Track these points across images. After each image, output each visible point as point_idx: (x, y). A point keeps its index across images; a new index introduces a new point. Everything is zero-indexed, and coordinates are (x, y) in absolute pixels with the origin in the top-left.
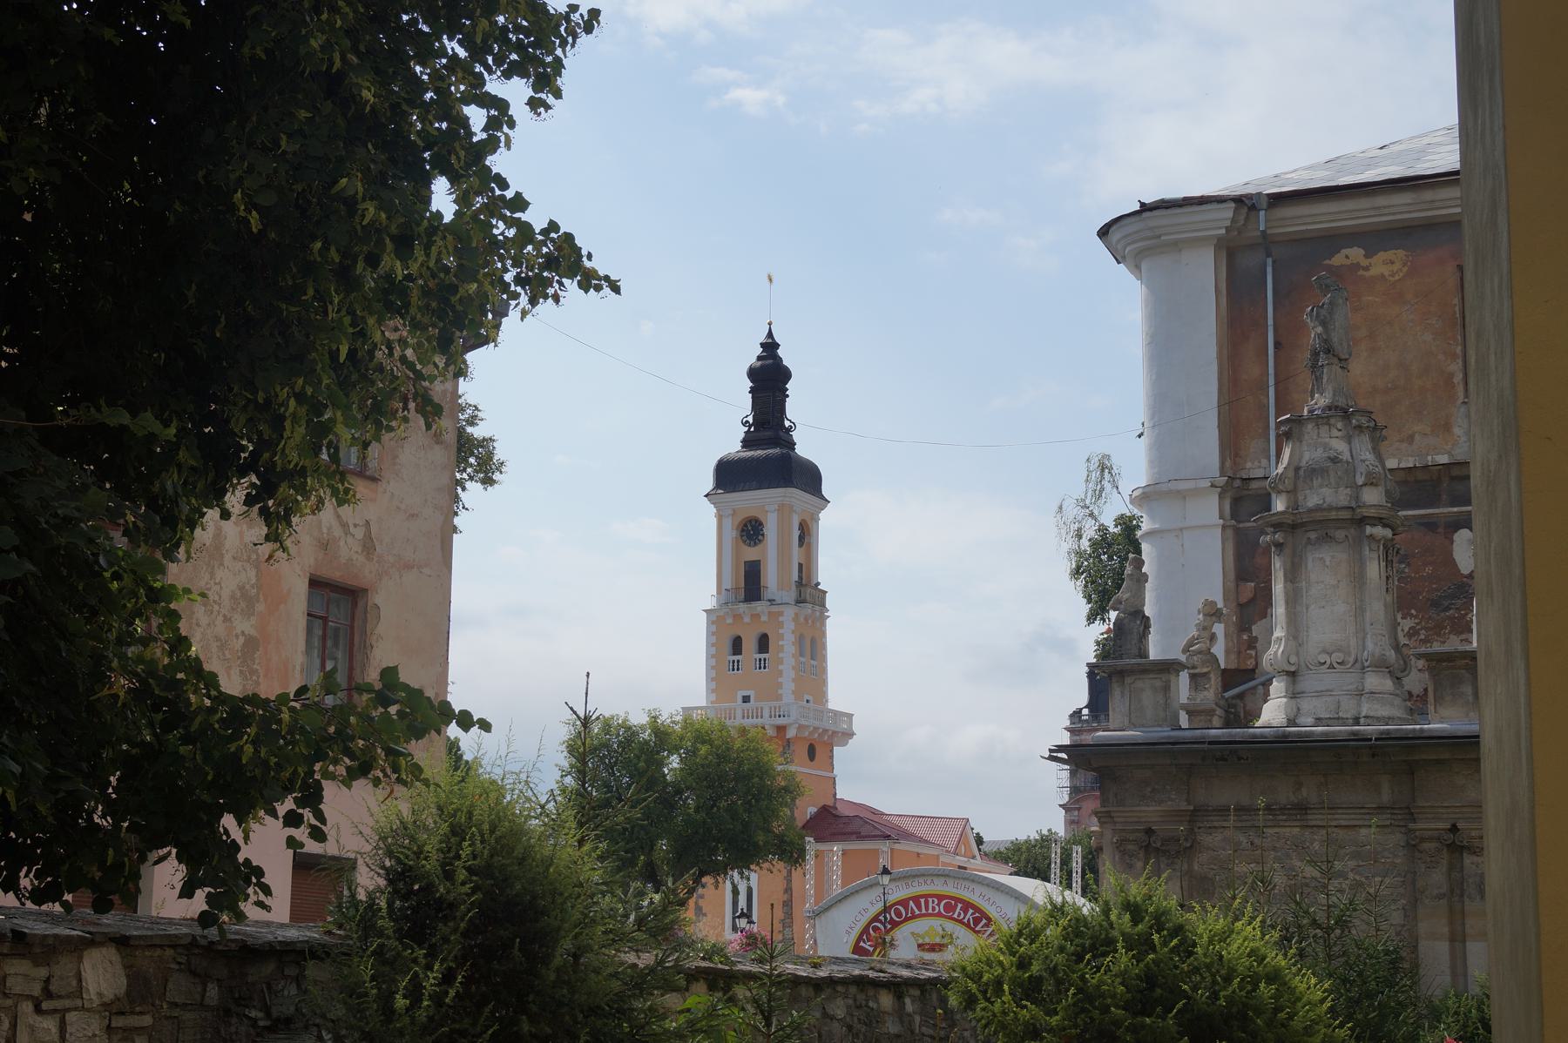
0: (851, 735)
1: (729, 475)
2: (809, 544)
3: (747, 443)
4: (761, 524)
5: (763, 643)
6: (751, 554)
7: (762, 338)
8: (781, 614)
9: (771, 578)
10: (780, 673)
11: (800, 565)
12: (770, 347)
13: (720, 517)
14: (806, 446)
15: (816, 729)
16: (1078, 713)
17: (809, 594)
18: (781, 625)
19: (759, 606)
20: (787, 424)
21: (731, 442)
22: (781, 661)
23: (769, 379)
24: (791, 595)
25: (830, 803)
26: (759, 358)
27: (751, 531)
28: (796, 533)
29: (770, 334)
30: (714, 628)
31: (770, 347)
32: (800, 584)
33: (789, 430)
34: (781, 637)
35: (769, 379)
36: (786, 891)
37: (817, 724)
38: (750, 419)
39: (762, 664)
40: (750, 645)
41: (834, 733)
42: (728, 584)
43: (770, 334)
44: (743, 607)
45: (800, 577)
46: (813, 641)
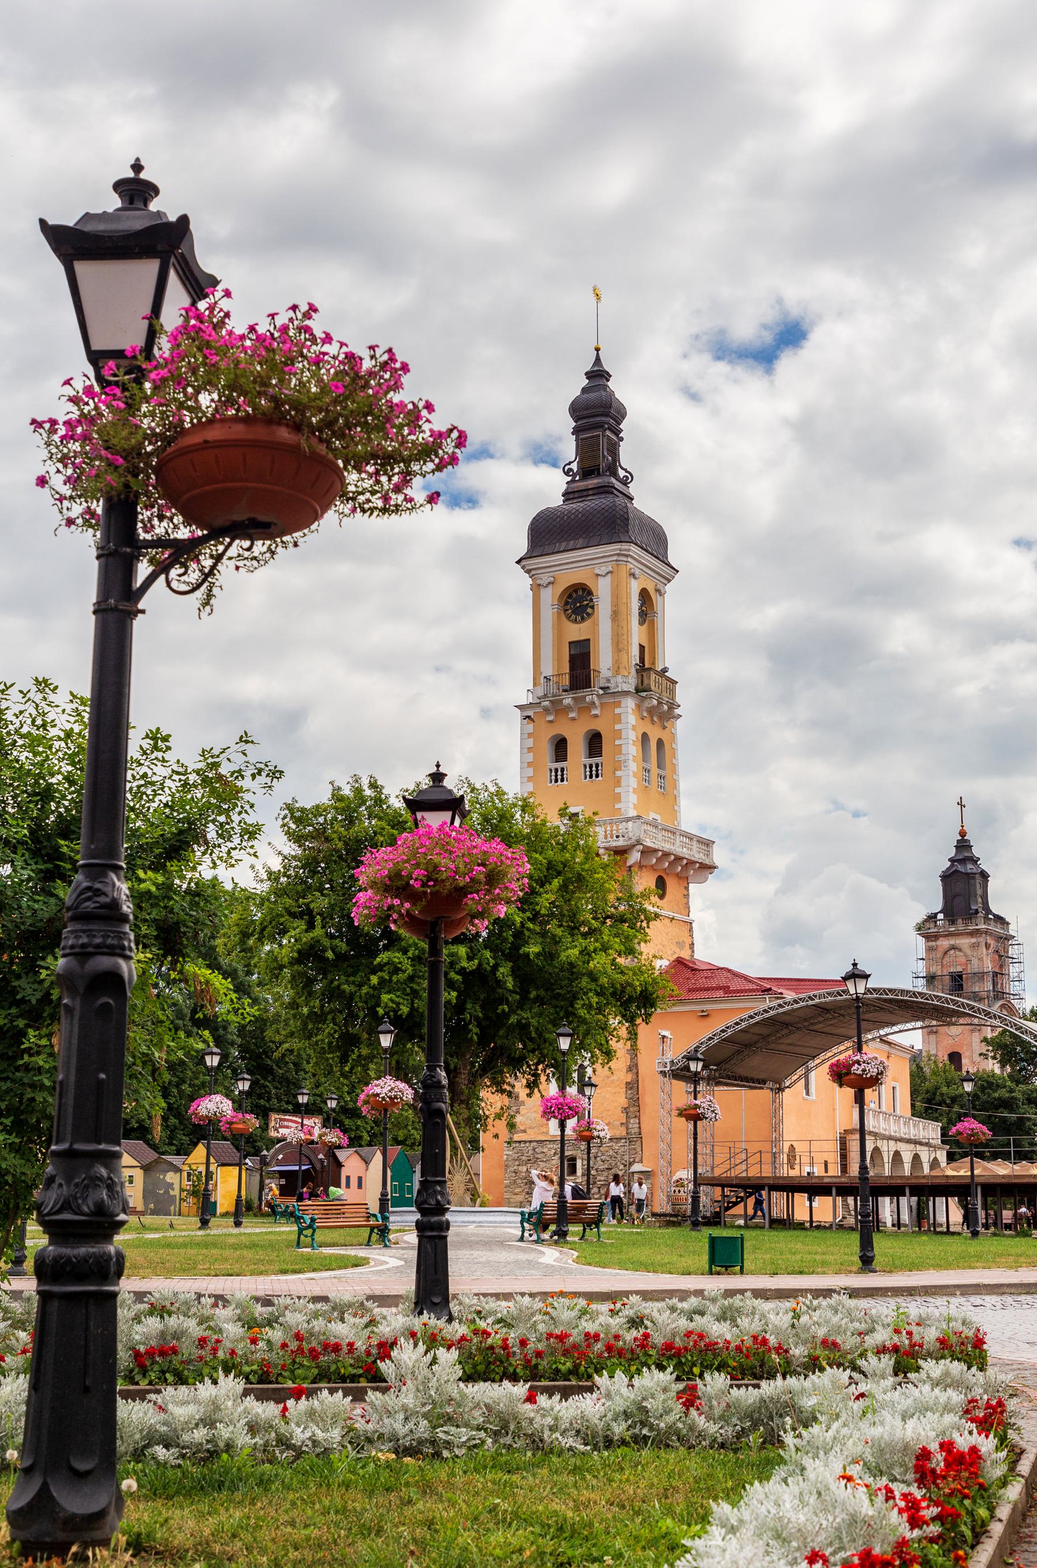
0: (710, 868)
1: (548, 534)
2: (652, 624)
3: (568, 495)
4: (590, 593)
5: (595, 743)
6: (576, 631)
8: (618, 704)
9: (603, 661)
10: (618, 782)
11: (642, 648)
12: (598, 375)
13: (536, 588)
14: (645, 500)
15: (666, 854)
16: (932, 917)
17: (653, 688)
18: (618, 719)
19: (591, 696)
20: (622, 473)
22: (617, 766)
23: (597, 417)
24: (629, 683)
25: (685, 954)
26: (584, 390)
27: (577, 602)
28: (635, 604)
29: (598, 359)
31: (598, 375)
32: (642, 669)
33: (625, 482)
34: (618, 734)
36: (630, 1069)
37: (667, 847)
38: (574, 467)
39: (593, 772)
40: (577, 749)
41: (691, 862)
42: (548, 670)
43: (598, 359)
44: (568, 701)
45: (642, 659)
46: (660, 743)
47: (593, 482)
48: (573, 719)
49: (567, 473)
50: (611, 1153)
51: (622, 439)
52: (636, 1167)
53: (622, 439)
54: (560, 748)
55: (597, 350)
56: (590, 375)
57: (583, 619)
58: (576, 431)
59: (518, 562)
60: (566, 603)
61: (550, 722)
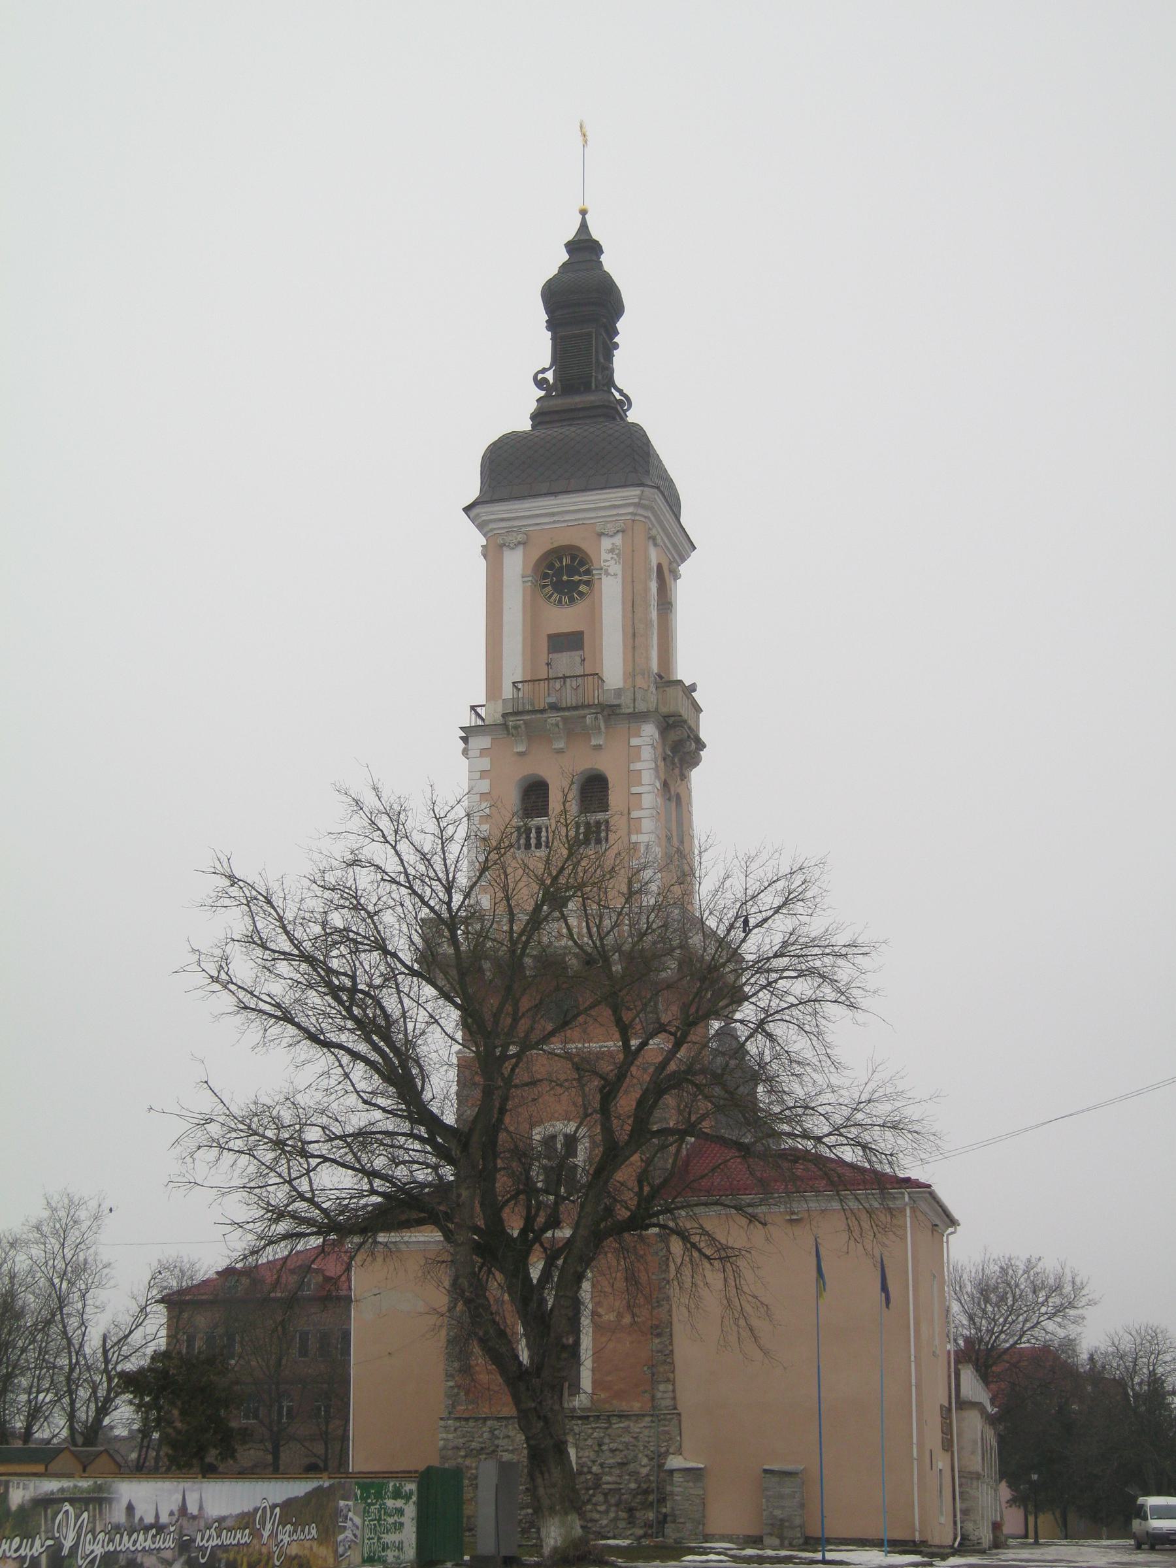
5: (594, 789)
6: (563, 619)
7: (570, 234)
12: (584, 248)
18: (633, 754)
21: (516, 410)
23: (583, 305)
26: (564, 267)
27: (563, 574)
29: (584, 226)
30: (485, 763)
31: (584, 248)
34: (633, 777)
35: (583, 305)
38: (549, 376)
43: (584, 226)
47: (577, 400)
48: (560, 752)
49: (540, 383)
50: (627, 1439)
51: (616, 346)
52: (674, 1462)
53: (616, 346)
54: (534, 795)
55: (584, 212)
56: (571, 246)
57: (572, 600)
58: (551, 325)
59: (467, 510)
60: (545, 576)
61: (521, 754)
